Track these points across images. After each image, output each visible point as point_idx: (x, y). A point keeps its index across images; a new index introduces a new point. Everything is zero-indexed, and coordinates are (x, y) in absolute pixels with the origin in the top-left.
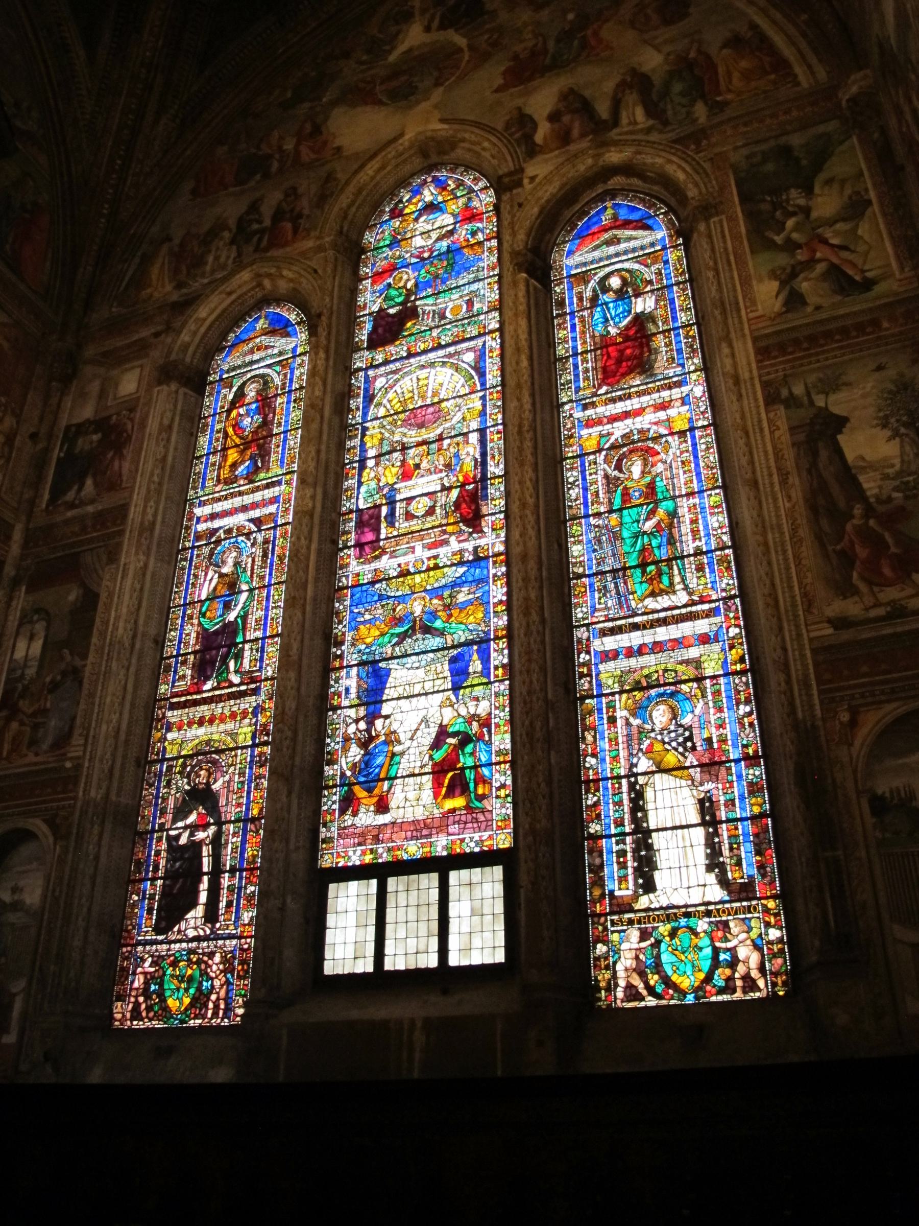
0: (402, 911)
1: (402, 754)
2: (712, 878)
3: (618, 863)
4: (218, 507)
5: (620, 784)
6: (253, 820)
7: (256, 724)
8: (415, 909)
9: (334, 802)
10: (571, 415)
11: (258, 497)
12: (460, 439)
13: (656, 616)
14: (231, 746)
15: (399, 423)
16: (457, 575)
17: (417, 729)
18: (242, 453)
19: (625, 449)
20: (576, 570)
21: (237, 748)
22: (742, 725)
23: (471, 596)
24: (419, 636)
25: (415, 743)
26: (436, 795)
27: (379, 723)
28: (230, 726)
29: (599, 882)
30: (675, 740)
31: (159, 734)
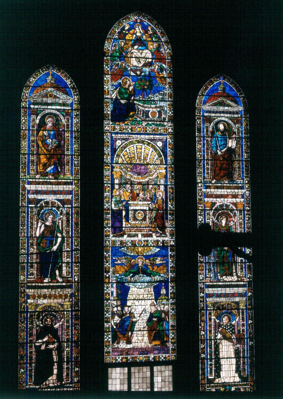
0: (137, 379)
1: (136, 322)
2: (237, 375)
3: (210, 368)
4: (40, 187)
5: (212, 342)
6: (75, 342)
7: (72, 301)
8: (141, 379)
9: (110, 338)
10: (201, 190)
11: (61, 188)
12: (156, 186)
13: (226, 283)
14: (61, 309)
15: (129, 169)
16: (156, 251)
17: (142, 313)
18: (49, 159)
19: (220, 212)
20: (200, 259)
21: (64, 311)
22: (249, 326)
23: (161, 262)
24: (141, 275)
25: (141, 319)
26: (149, 339)
27: (126, 308)
28: (60, 301)
29: (203, 374)
30: (229, 329)
31: (23, 299)
